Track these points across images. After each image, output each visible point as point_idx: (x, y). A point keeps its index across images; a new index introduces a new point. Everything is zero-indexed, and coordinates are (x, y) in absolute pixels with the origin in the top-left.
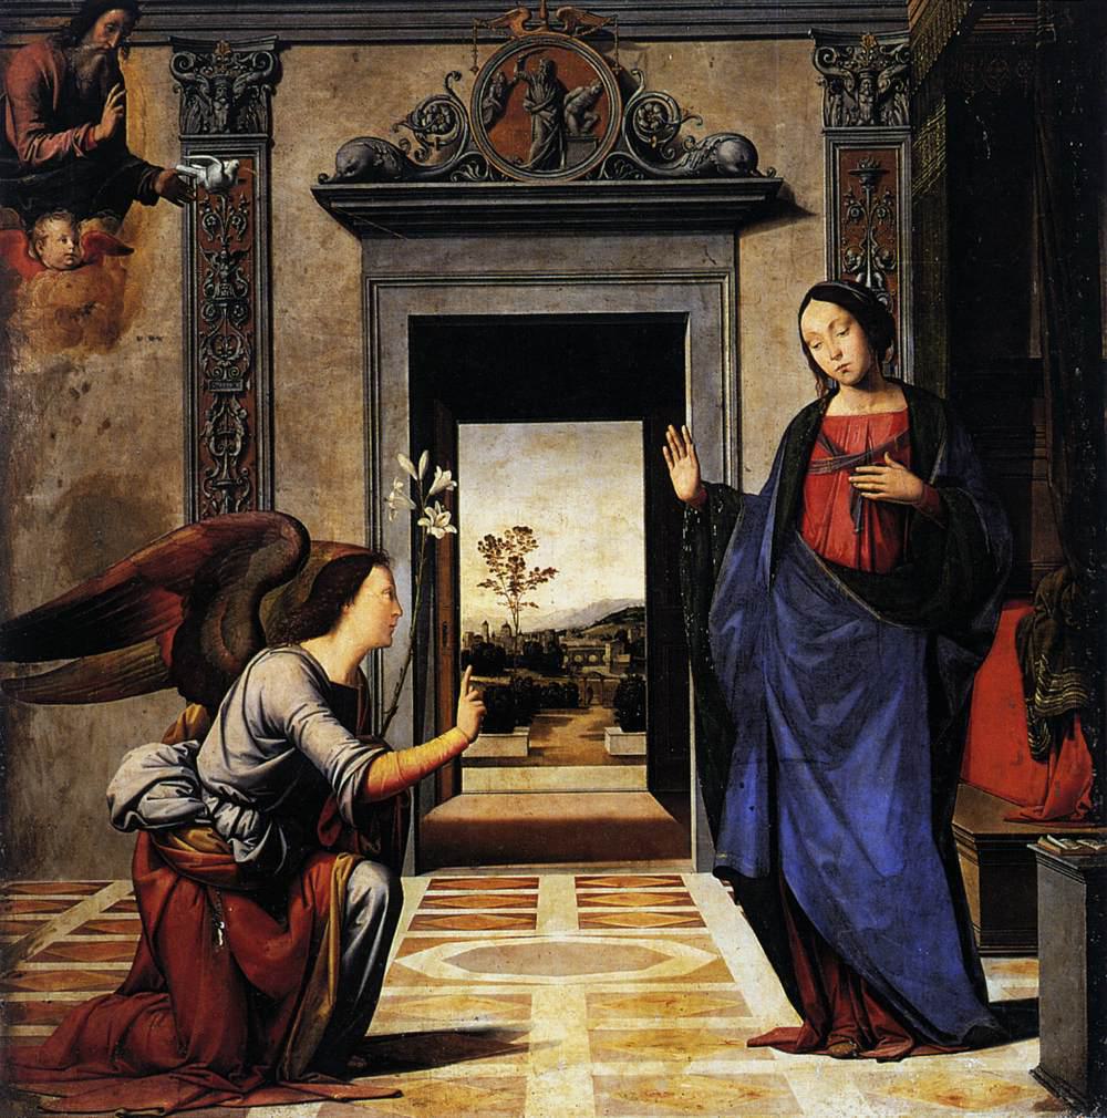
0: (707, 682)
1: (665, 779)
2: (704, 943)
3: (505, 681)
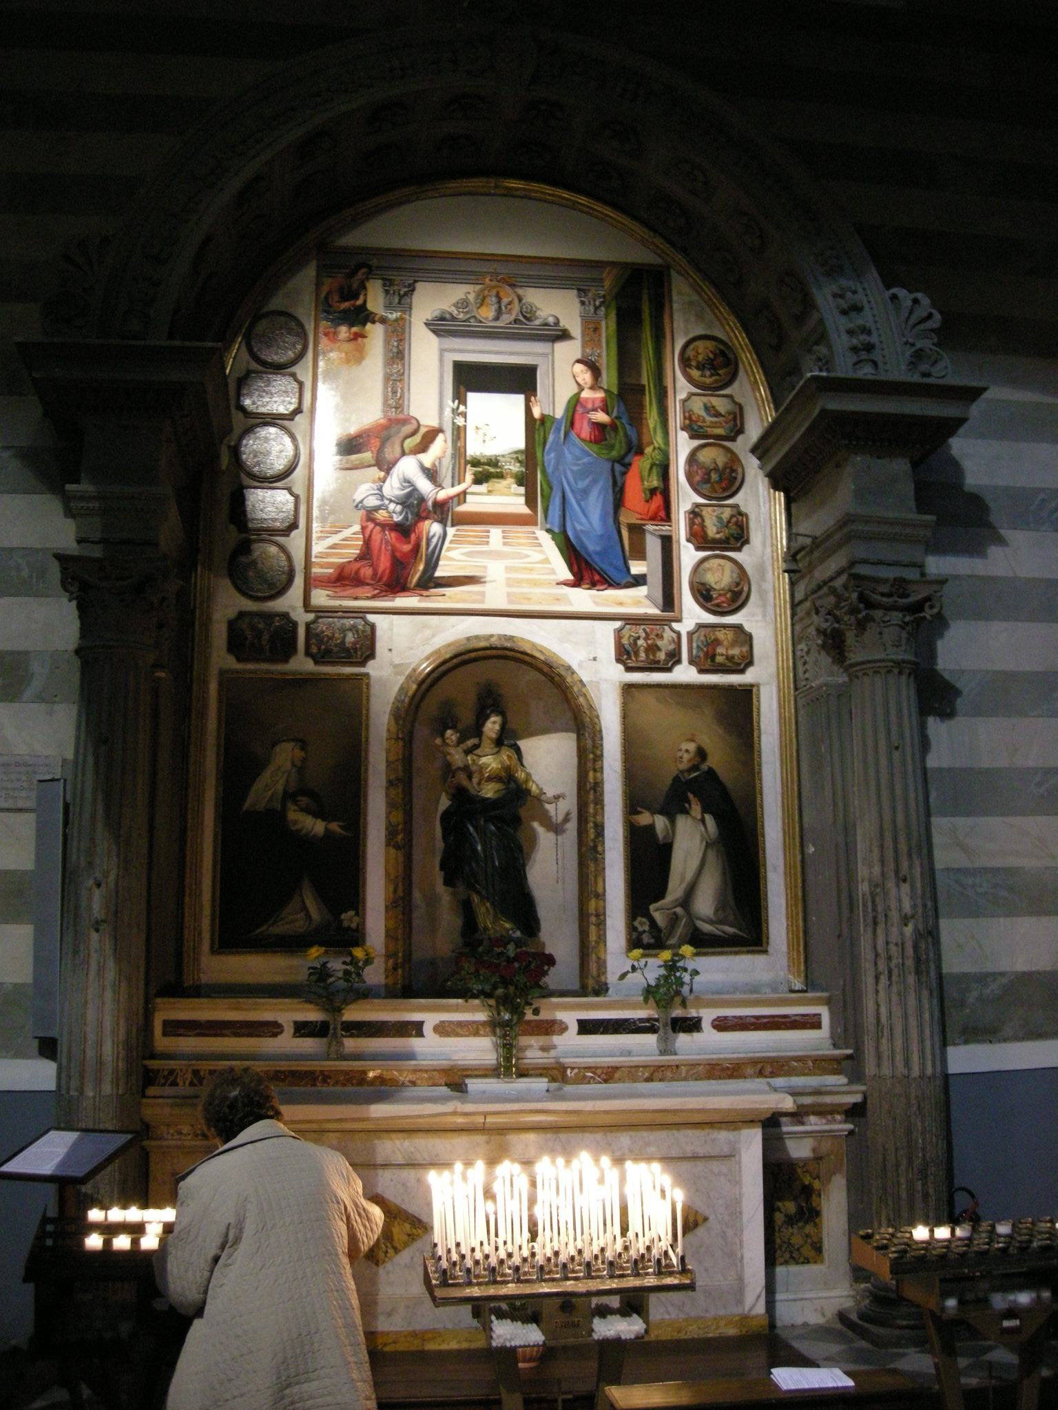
0: (544, 472)
1: (530, 501)
2: (542, 552)
3: (480, 469)
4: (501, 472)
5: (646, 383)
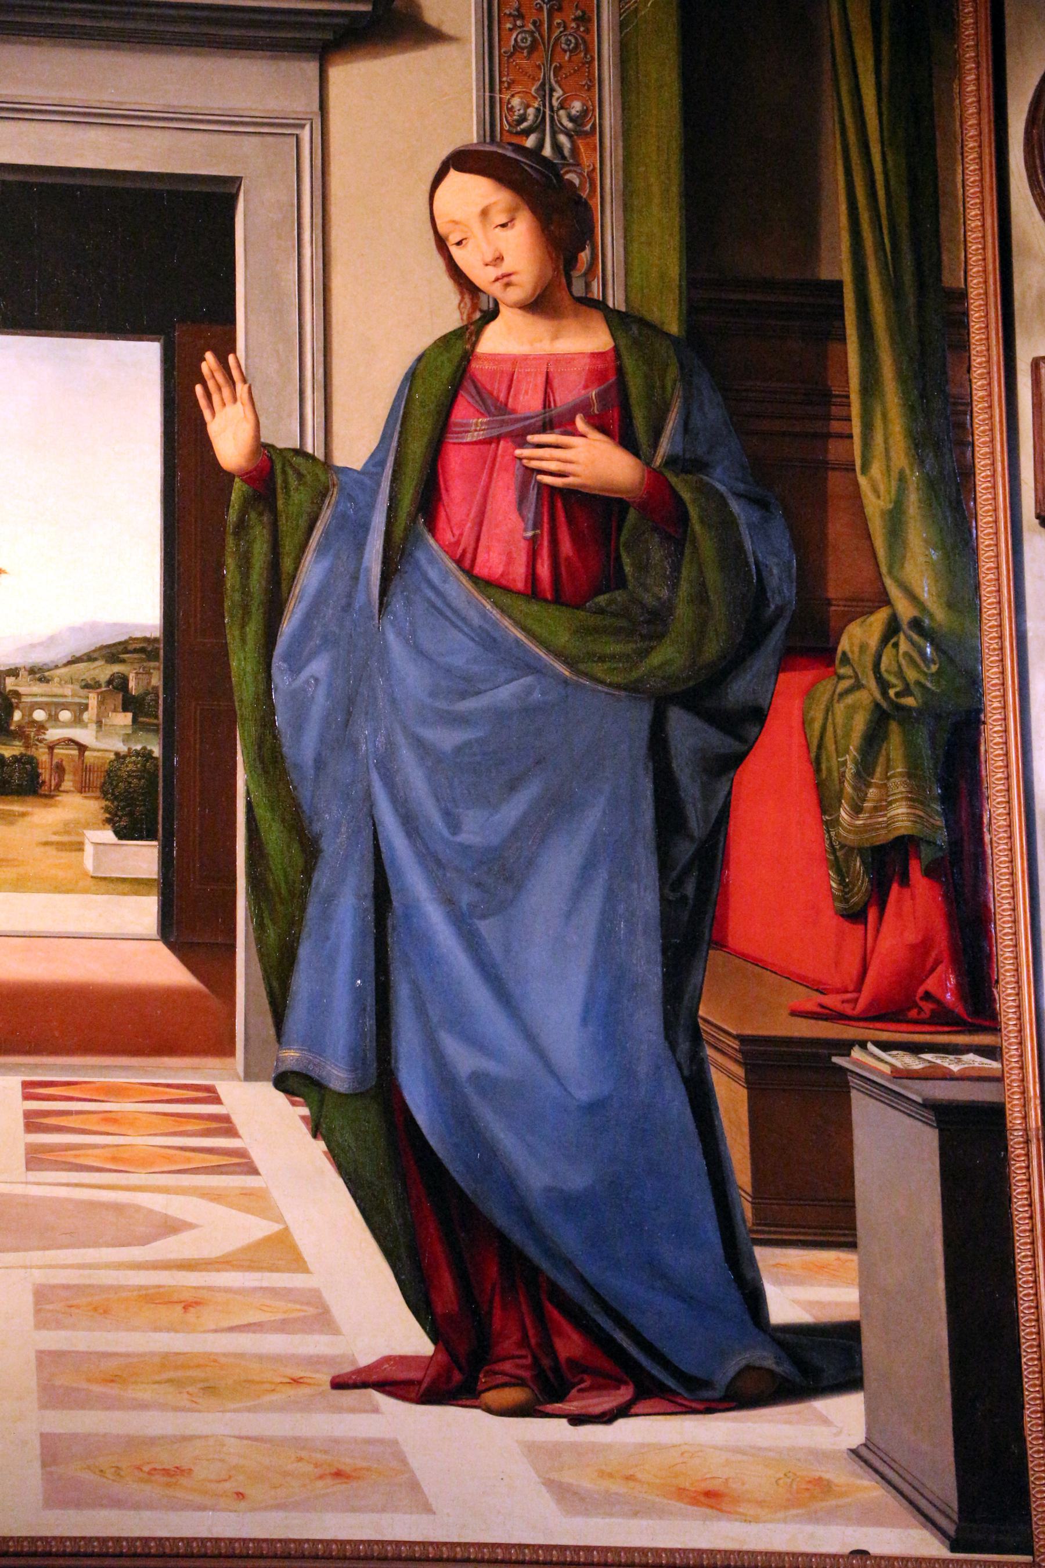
4: (27, 763)
5: (846, 275)
